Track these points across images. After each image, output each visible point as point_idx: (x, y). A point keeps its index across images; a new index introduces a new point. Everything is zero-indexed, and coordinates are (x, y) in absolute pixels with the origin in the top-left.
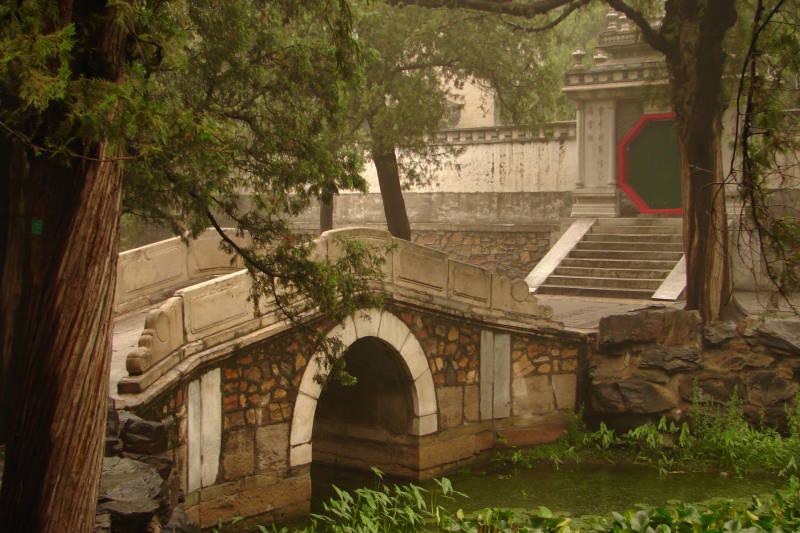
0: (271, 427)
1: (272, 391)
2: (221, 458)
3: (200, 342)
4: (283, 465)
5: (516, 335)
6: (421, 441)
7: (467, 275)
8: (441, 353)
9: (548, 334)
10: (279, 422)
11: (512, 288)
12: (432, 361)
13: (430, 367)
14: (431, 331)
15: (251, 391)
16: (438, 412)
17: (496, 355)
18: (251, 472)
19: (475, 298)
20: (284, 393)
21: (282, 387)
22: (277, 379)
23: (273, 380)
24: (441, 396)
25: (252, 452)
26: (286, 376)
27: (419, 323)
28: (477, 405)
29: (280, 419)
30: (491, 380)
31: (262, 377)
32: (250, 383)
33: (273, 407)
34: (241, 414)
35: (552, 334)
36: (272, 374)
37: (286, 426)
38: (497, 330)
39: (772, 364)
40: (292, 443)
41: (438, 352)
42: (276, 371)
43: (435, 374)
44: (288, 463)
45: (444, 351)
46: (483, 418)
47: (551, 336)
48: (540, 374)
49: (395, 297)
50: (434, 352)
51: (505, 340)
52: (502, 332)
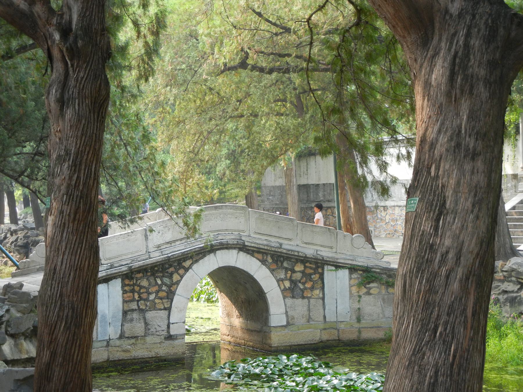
0: (156, 311)
1: (157, 292)
2: (122, 325)
3: (109, 264)
4: (165, 333)
5: (353, 269)
6: (272, 329)
7: (313, 231)
8: (288, 278)
9: (377, 269)
10: (161, 310)
11: (352, 239)
12: (281, 282)
13: (279, 285)
14: (280, 264)
15: (142, 291)
16: (286, 312)
17: (338, 281)
18: (143, 335)
19: (322, 246)
20: (164, 294)
21: (163, 291)
22: (160, 286)
23: (157, 287)
24: (288, 304)
25: (143, 324)
26: (166, 285)
27: (270, 260)
28: (322, 311)
29: (162, 308)
30: (335, 297)
31: (150, 285)
32: (141, 287)
33: (157, 301)
34: (136, 303)
35: (379, 269)
36: (156, 284)
37: (166, 312)
38: (338, 266)
39: (518, 289)
40: (171, 322)
41: (286, 277)
42: (159, 282)
43: (284, 291)
44: (168, 332)
45: (291, 277)
46: (327, 320)
47: (378, 270)
48: (370, 294)
49: (246, 244)
50: (283, 276)
51: (347, 272)
52: (343, 267)
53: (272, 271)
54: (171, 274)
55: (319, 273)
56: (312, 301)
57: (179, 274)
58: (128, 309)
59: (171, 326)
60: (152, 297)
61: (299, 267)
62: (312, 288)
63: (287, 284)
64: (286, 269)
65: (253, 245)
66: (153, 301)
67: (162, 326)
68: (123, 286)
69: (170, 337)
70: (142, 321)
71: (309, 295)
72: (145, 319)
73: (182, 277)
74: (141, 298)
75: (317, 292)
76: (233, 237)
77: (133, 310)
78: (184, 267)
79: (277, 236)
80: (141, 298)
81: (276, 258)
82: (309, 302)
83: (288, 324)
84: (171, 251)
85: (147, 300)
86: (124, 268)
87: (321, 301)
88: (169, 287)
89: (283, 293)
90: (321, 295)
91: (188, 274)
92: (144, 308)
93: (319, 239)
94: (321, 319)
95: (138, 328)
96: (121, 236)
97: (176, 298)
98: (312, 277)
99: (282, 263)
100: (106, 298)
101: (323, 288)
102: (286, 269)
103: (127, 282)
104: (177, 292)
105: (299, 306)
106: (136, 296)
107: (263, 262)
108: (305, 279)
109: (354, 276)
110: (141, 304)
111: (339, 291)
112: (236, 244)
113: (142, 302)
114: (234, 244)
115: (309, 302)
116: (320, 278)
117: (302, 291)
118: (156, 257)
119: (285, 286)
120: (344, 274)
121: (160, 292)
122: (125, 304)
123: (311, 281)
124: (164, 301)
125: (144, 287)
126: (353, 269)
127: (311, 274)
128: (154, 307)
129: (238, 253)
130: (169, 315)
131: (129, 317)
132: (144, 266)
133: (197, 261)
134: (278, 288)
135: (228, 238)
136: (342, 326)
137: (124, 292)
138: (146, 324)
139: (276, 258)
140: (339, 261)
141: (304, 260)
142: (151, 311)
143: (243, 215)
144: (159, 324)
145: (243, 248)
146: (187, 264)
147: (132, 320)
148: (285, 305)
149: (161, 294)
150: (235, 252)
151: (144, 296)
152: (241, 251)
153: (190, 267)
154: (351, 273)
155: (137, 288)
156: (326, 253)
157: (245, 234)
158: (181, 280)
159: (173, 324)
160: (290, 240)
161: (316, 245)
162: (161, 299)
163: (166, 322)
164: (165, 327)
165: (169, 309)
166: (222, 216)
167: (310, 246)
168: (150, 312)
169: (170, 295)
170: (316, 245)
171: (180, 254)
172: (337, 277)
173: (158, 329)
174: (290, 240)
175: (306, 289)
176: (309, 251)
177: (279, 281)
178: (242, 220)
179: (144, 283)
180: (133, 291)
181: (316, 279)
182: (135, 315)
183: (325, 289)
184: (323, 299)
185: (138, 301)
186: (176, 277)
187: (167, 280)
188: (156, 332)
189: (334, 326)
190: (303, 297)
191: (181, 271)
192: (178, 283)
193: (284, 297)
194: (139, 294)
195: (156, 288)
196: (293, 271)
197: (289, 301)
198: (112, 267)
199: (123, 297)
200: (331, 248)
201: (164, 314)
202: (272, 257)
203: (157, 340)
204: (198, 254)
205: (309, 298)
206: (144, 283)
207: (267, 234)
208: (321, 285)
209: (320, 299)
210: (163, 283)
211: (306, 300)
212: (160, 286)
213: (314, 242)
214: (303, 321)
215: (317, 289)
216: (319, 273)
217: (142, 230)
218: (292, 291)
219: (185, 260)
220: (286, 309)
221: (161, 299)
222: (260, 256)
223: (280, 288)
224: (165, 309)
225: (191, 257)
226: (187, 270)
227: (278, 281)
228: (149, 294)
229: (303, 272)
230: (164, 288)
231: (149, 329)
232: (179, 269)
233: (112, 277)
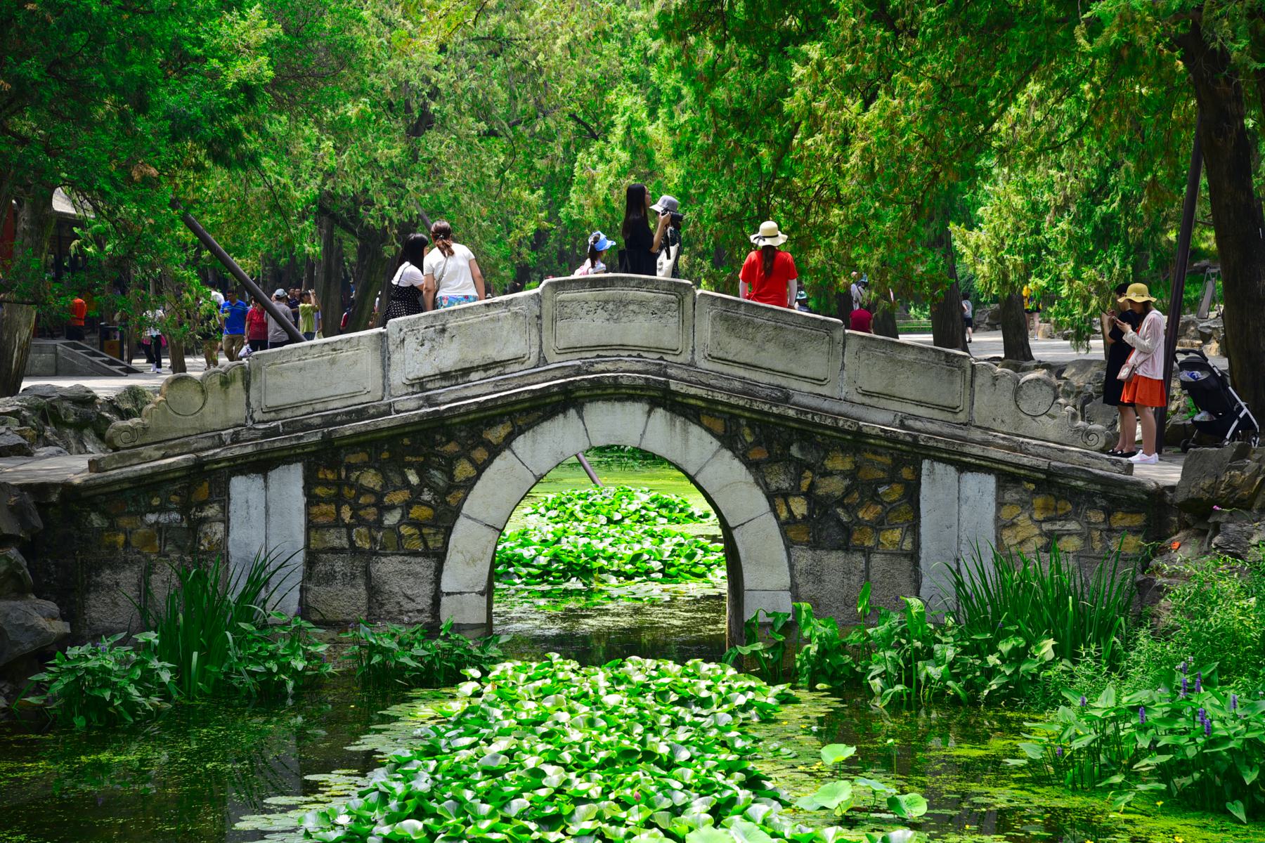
0: (400, 558)
1: (408, 505)
7: (892, 360)
8: (804, 488)
10: (415, 554)
12: (779, 501)
13: (774, 509)
14: (777, 449)
15: (362, 500)
17: (964, 507)
19: (919, 403)
25: (362, 590)
26: (433, 489)
33: (405, 530)
35: (1083, 479)
36: (407, 484)
40: (445, 587)
42: (413, 479)
45: (812, 485)
49: (674, 386)
51: (990, 481)
55: (902, 481)
56: (877, 559)
57: (471, 461)
58: (321, 546)
59: (444, 600)
60: (392, 519)
61: (840, 463)
62: (878, 525)
63: (799, 507)
65: (693, 391)
66: (394, 529)
67: (418, 600)
70: (360, 581)
71: (869, 543)
72: (367, 574)
73: (481, 469)
74: (359, 521)
76: (639, 367)
77: (334, 550)
78: (487, 445)
79: (780, 368)
80: (359, 521)
82: (868, 562)
84: (453, 396)
85: (379, 524)
86: (314, 437)
87: (906, 564)
88: (442, 493)
89: (784, 534)
90: (908, 545)
91: (498, 463)
92: (367, 546)
93: (909, 384)
96: (313, 351)
97: (461, 526)
98: (881, 490)
99: (787, 446)
100: (257, 513)
101: (914, 527)
102: (801, 466)
104: (466, 509)
106: (346, 514)
107: (728, 440)
108: (856, 495)
109: (1010, 496)
110: (359, 535)
111: (964, 538)
112: (642, 388)
113: (363, 530)
114: (634, 387)
115: (868, 562)
116: (904, 496)
118: (409, 407)
119: (790, 511)
120: (981, 487)
121: (415, 508)
122: (312, 533)
123: (877, 503)
124: (425, 531)
125: (371, 491)
126: (1008, 477)
128: (399, 547)
129: (649, 413)
130: (439, 571)
131: (321, 568)
132: (367, 433)
133: (530, 426)
134: (771, 516)
135: (627, 369)
137: (312, 500)
140: (967, 449)
142: (386, 555)
143: (674, 306)
144: (409, 592)
146: (497, 434)
148: (791, 567)
150: (639, 409)
151: (370, 514)
152: (659, 406)
154: (1000, 487)
155: (349, 493)
156: (929, 424)
157: (680, 359)
158: (478, 477)
159: (448, 594)
161: (902, 399)
162: (417, 524)
163: (428, 589)
164: (425, 602)
165: (439, 557)
166: (610, 306)
167: (883, 403)
168: (384, 559)
169: (445, 519)
170: (902, 399)
171: (474, 407)
172: (962, 496)
173: (408, 606)
175: (859, 522)
176: (879, 420)
180: (338, 500)
181: (894, 497)
183: (922, 530)
185: (349, 527)
186: (463, 470)
188: (401, 612)
190: (846, 548)
191: (480, 454)
192: (469, 484)
193: (789, 544)
194: (355, 509)
195: (400, 497)
197: (804, 558)
199: (308, 514)
200: (953, 410)
201: (423, 567)
204: (527, 411)
205: (867, 553)
207: (748, 361)
208: (910, 517)
209: (905, 556)
211: (858, 559)
212: (416, 491)
213: (895, 391)
215: (893, 527)
216: (902, 481)
217: (372, 336)
219: (491, 422)
220: (792, 577)
221: (417, 524)
223: (777, 517)
224: (426, 554)
226: (494, 451)
227: (771, 496)
228: (384, 509)
231: (382, 605)
232: (474, 448)
233: (277, 459)
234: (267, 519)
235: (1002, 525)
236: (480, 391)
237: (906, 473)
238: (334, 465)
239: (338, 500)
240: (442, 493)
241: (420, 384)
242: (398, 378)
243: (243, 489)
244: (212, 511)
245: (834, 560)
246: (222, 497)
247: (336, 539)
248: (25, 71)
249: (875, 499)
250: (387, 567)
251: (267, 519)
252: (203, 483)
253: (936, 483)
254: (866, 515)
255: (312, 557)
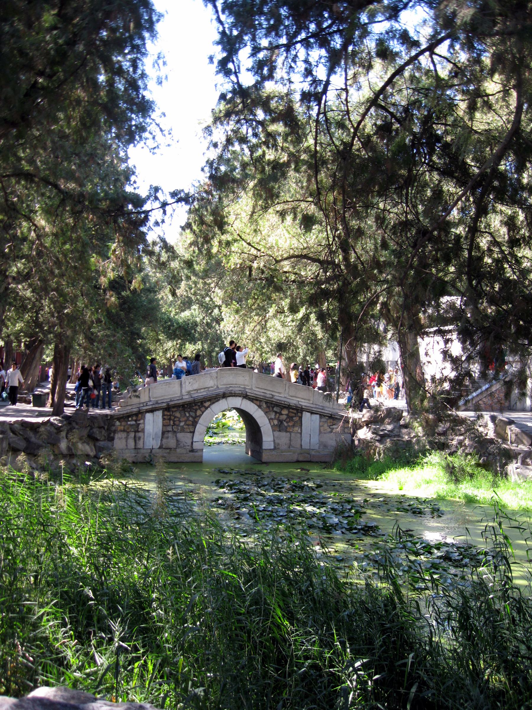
1: (185, 421)
27: (264, 405)
32: (175, 417)
50: (273, 417)
51: (318, 416)
53: (266, 413)
54: (196, 410)
60: (182, 424)
61: (285, 412)
62: (294, 426)
63: (276, 422)
64: (276, 412)
66: (182, 427)
68: (163, 415)
69: (192, 451)
74: (174, 424)
75: (296, 429)
81: (270, 405)
83: (275, 448)
85: (178, 425)
86: (165, 404)
87: (299, 435)
88: (194, 418)
94: (299, 446)
95: (171, 442)
100: (151, 422)
102: (276, 412)
103: (166, 413)
105: (283, 438)
106: (172, 423)
107: (260, 406)
109: (323, 420)
117: (286, 427)
118: (187, 398)
126: (322, 416)
127: (292, 417)
128: (183, 430)
131: (166, 435)
135: (237, 390)
136: (313, 453)
137: (164, 419)
138: (177, 441)
139: (270, 405)
141: (288, 407)
145: (246, 396)
146: (207, 404)
147: (167, 438)
149: (188, 423)
150: (240, 399)
151: (177, 423)
153: (209, 407)
154: (321, 418)
156: (304, 403)
160: (279, 393)
169: (195, 424)
174: (279, 393)
176: (293, 402)
177: (270, 420)
178: (247, 378)
179: (178, 414)
180: (170, 419)
182: (170, 435)
184: (301, 433)
186: (199, 413)
187: (192, 414)
189: (308, 452)
190: (286, 431)
191: (203, 409)
192: (200, 416)
194: (174, 421)
196: (281, 414)
197: (277, 433)
198: (157, 403)
201: (189, 435)
202: (266, 403)
203: (183, 451)
205: (290, 432)
206: (178, 414)
210: (190, 416)
212: (188, 417)
214: (285, 447)
218: (279, 427)
222: (258, 403)
225: (209, 400)
226: (207, 408)
229: (287, 415)
230: (191, 419)
234: (153, 424)
235: (320, 426)
236: (203, 393)
237: (299, 414)
238: (169, 411)
239: (170, 419)
240: (194, 418)
241: (189, 393)
242: (183, 391)
243: (148, 416)
244: (142, 421)
245: (283, 434)
246: (144, 418)
247: (170, 428)
248: (175, 343)
249: (293, 420)
250: (180, 435)
251: (153, 424)
252: (139, 414)
253: (306, 416)
254: (290, 424)
255: (163, 433)
